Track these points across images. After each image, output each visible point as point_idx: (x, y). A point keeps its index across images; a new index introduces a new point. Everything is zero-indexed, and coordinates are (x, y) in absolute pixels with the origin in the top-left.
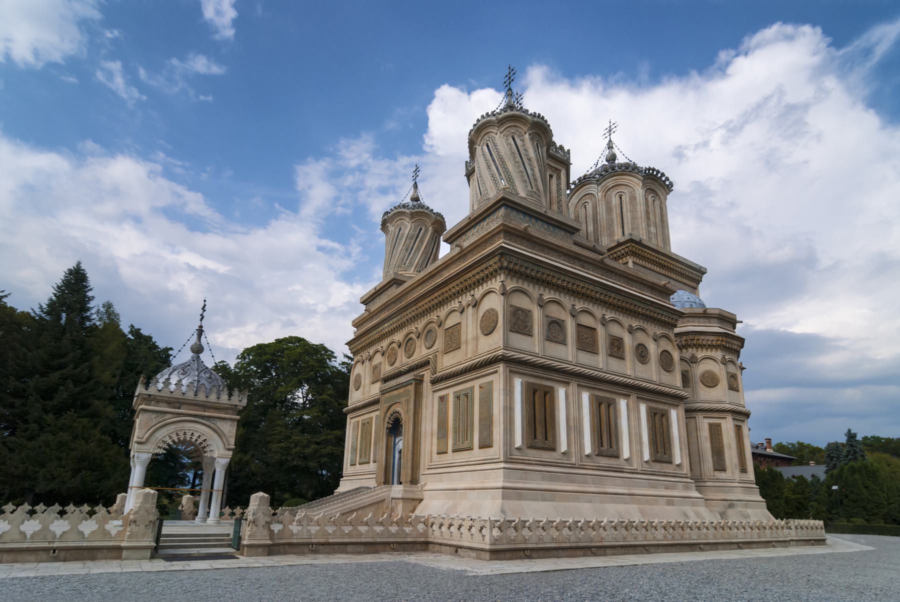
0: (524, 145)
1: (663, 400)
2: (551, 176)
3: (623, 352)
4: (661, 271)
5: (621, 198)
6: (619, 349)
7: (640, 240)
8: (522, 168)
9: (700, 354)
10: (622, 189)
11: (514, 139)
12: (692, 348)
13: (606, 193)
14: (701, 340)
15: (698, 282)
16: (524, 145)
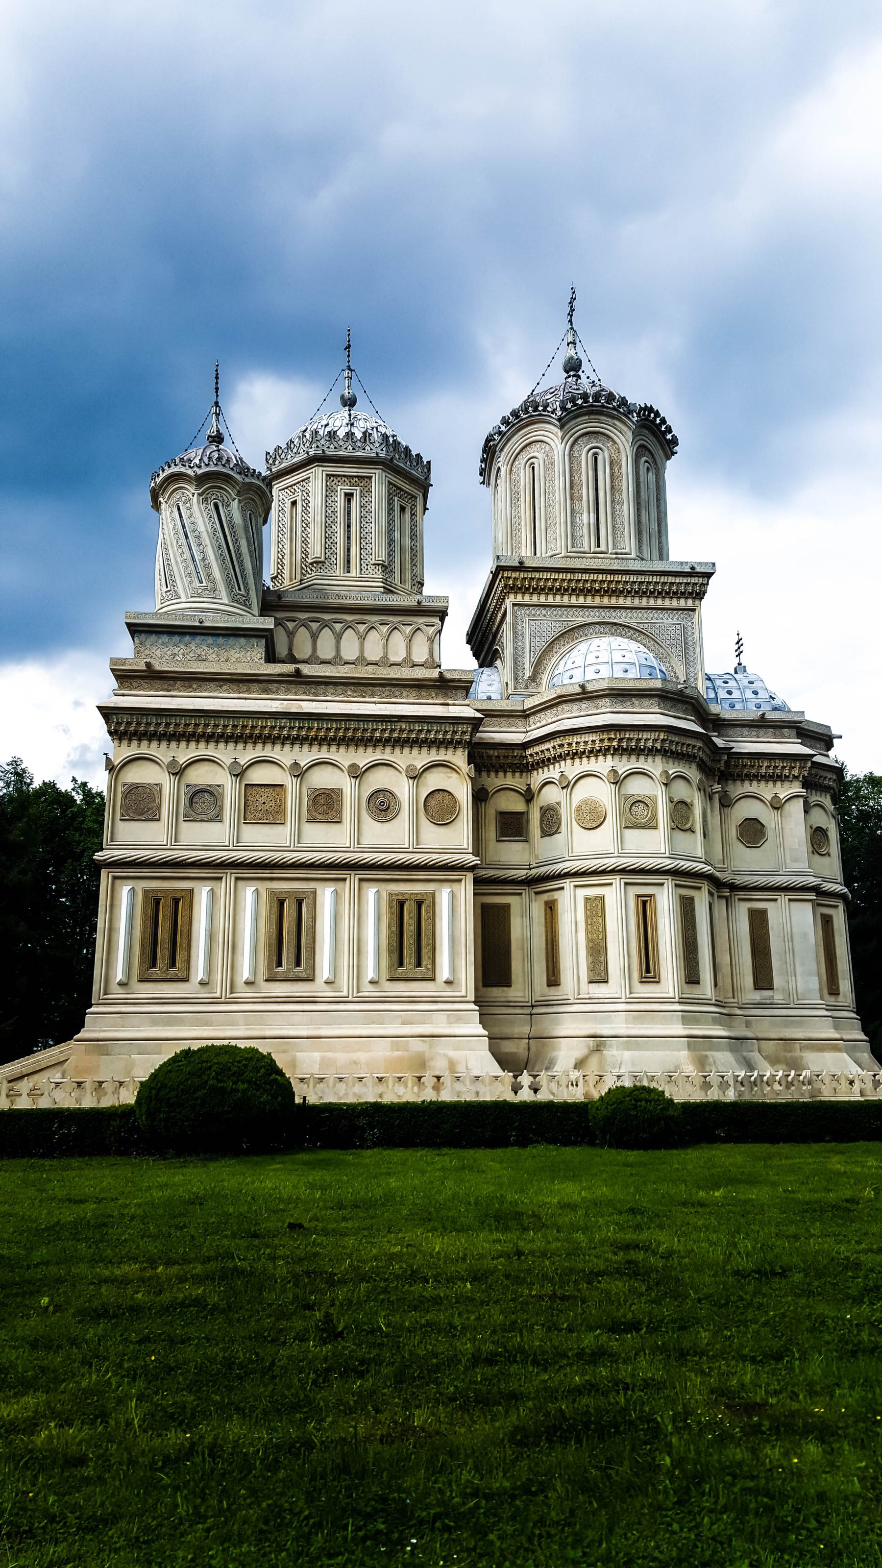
0: (191, 516)
1: (422, 875)
2: (349, 496)
3: (340, 812)
4: (589, 601)
5: (533, 468)
6: (330, 807)
7: (521, 563)
8: (187, 554)
9: (571, 769)
10: (533, 451)
11: (179, 509)
12: (565, 760)
13: (512, 465)
14: (574, 744)
15: (700, 595)
16: (191, 516)
